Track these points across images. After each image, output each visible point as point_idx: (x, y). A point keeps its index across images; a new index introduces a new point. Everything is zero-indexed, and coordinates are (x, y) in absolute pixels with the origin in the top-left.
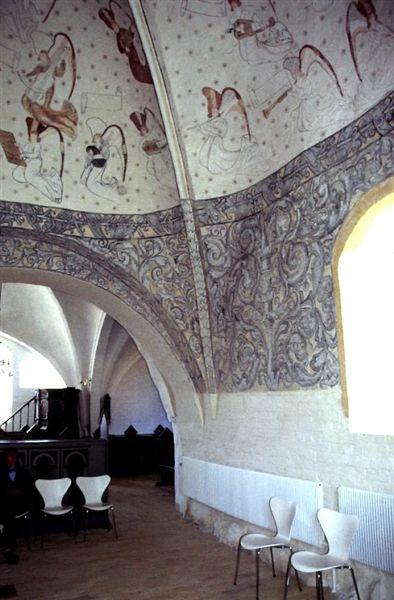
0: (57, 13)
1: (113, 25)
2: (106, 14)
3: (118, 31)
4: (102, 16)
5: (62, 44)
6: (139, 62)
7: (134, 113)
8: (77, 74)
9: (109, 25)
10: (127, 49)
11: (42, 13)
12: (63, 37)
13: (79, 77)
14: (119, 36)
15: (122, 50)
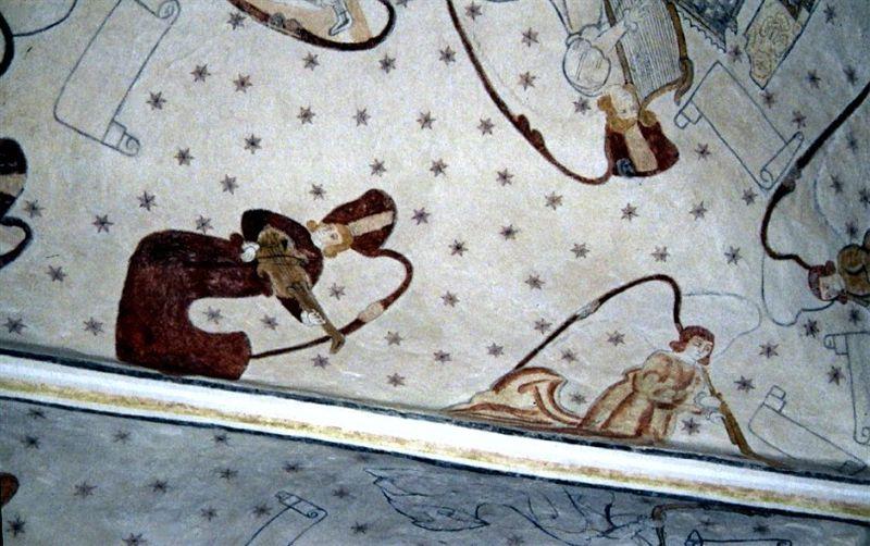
0: (448, 56)
1: (336, 229)
2: (375, 223)
3: (321, 239)
4: (376, 202)
5: (360, 19)
6: (205, 292)
7: (22, 167)
8: (248, 20)
9: (343, 215)
10: (250, 251)
11: (473, 11)
12: (376, 33)
13: (236, 21)
14: (300, 234)
15: (255, 221)
